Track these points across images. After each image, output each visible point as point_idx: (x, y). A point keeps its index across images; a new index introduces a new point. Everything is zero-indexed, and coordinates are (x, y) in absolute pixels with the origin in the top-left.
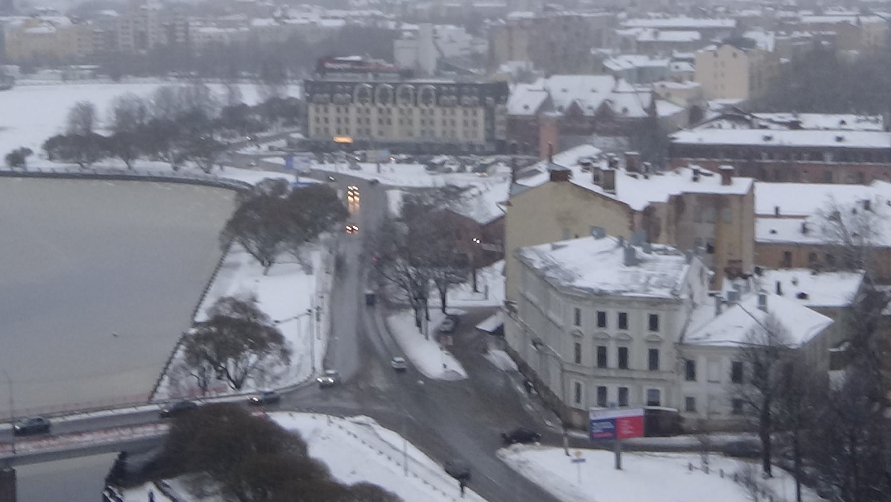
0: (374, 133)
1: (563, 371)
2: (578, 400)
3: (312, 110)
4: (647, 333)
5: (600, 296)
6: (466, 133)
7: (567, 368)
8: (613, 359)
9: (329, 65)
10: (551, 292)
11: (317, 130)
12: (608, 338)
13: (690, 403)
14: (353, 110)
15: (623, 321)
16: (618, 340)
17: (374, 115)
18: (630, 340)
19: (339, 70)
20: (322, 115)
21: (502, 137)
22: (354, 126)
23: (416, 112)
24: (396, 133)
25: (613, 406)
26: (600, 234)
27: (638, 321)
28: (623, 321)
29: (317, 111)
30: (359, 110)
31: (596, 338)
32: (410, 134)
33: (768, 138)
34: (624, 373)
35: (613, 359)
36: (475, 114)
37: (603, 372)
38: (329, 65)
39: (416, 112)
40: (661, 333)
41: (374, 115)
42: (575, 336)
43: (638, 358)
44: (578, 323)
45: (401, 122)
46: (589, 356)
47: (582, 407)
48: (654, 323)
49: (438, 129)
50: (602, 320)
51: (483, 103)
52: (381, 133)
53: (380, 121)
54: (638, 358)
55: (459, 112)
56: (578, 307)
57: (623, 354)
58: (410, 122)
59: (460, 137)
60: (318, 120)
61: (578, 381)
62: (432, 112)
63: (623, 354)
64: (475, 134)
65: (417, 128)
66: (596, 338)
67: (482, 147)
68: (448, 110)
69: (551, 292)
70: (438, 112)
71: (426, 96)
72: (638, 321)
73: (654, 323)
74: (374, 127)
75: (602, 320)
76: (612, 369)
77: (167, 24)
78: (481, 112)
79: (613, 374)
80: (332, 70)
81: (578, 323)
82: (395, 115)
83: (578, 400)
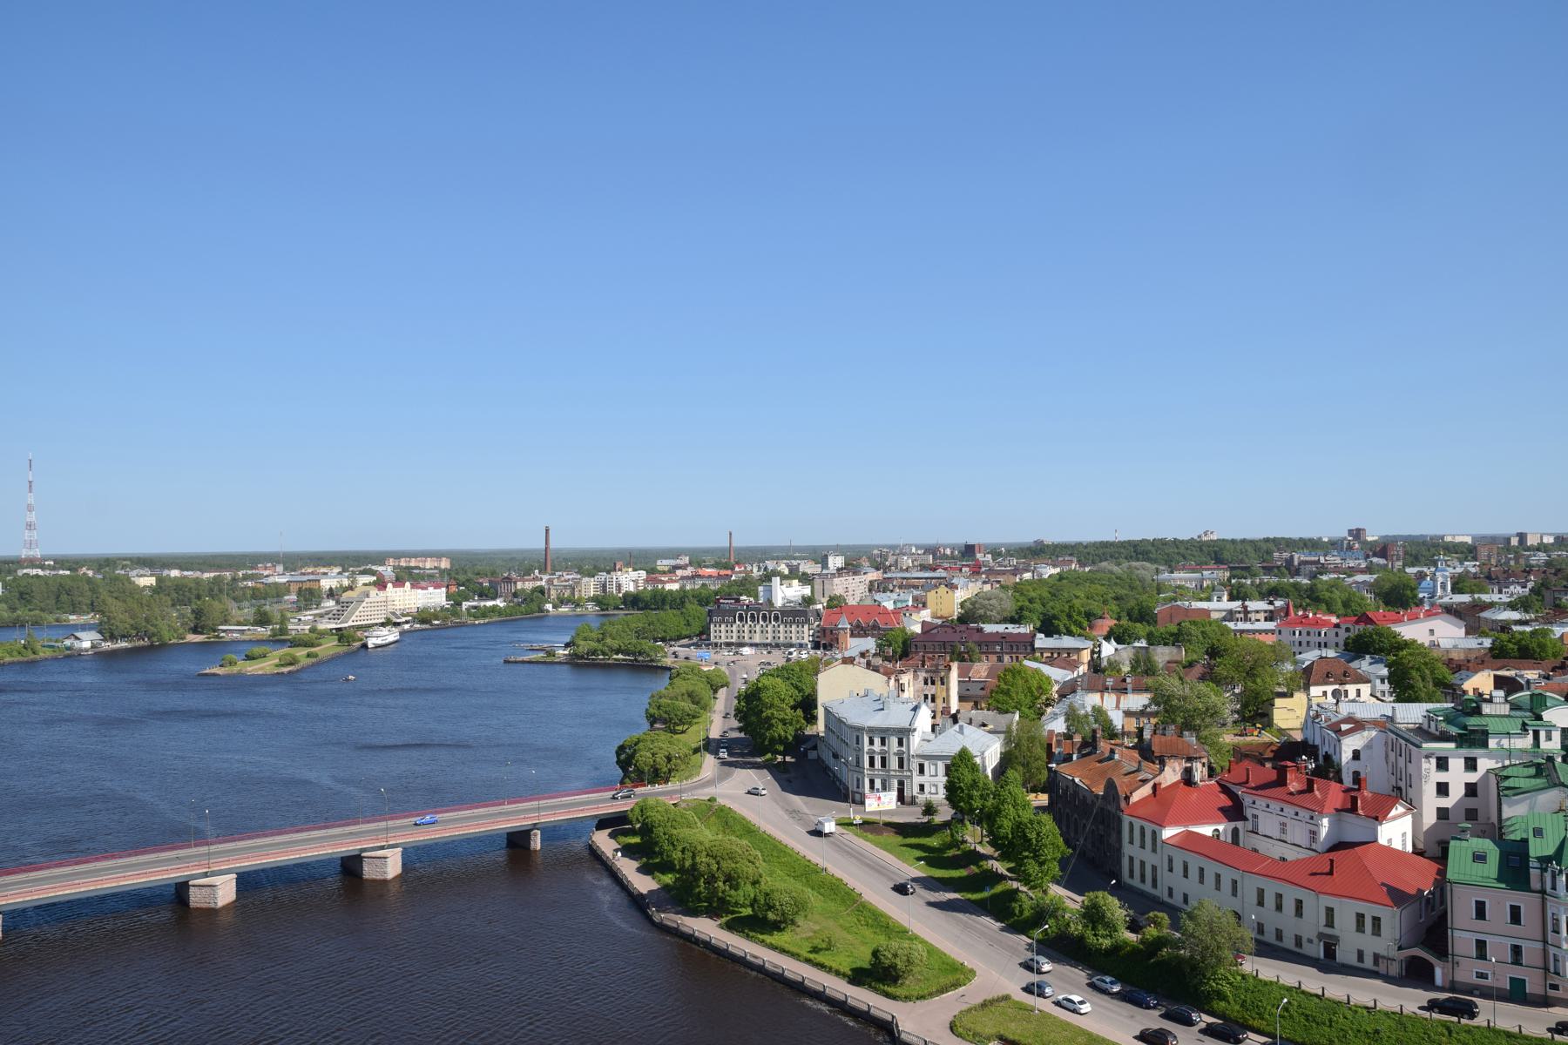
2: (858, 787)
3: (712, 626)
8: (878, 764)
9: (721, 601)
13: (922, 787)
16: (880, 753)
17: (746, 628)
22: (735, 635)
24: (757, 639)
25: (878, 790)
35: (878, 764)
38: (721, 601)
43: (894, 763)
44: (858, 743)
45: (762, 632)
47: (860, 791)
53: (750, 632)
54: (894, 763)
59: (794, 641)
62: (779, 626)
65: (770, 635)
81: (858, 743)
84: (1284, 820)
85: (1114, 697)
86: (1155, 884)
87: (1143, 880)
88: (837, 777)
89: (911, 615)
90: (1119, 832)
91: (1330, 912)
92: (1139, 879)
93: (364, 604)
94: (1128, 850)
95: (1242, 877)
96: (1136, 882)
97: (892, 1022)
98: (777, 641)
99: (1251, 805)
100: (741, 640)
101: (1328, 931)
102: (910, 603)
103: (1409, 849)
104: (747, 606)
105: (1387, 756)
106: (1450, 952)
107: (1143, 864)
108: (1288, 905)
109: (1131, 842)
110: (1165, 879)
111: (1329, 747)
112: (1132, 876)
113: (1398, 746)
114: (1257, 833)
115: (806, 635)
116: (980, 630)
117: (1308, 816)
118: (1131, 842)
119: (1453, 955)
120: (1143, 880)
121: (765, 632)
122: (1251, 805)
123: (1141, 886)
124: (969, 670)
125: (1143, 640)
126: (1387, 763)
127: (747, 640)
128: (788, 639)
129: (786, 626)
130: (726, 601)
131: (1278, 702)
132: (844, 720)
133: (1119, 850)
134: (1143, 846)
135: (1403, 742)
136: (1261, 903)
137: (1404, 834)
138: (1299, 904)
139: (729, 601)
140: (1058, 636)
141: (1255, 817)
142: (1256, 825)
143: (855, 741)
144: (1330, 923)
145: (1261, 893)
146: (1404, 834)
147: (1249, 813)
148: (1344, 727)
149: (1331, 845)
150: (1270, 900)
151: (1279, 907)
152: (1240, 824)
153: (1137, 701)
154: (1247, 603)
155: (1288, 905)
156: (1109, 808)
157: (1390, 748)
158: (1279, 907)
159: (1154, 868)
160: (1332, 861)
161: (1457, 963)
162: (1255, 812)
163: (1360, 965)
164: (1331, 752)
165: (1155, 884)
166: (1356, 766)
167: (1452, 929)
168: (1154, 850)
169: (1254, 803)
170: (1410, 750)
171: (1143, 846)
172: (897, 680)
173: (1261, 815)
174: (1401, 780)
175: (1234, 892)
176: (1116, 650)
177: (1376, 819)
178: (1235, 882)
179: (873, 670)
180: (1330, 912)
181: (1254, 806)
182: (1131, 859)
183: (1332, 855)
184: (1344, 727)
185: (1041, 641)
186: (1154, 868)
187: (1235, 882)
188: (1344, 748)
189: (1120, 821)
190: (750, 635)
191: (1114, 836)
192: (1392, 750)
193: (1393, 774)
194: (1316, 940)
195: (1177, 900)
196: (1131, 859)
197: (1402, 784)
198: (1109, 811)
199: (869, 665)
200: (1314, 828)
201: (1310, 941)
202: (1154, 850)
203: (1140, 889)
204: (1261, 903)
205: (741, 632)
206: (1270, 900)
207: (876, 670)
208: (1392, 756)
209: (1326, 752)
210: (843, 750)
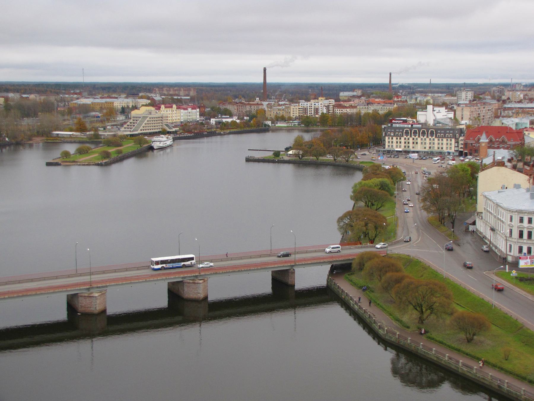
0: (411, 148)
1: (506, 240)
3: (387, 138)
5: (520, 212)
6: (447, 148)
7: (508, 239)
10: (500, 209)
11: (389, 146)
12: (524, 228)
14: (403, 138)
17: (411, 140)
19: (397, 123)
20: (390, 140)
21: (462, 150)
22: (403, 145)
23: (428, 139)
24: (419, 148)
25: (525, 254)
29: (389, 138)
30: (405, 139)
31: (518, 227)
32: (425, 148)
34: (529, 242)
36: (451, 140)
37: (521, 241)
38: (393, 121)
39: (428, 139)
41: (411, 140)
42: (510, 226)
45: (422, 143)
46: (516, 234)
47: (512, 254)
49: (436, 146)
50: (521, 220)
51: (454, 137)
52: (413, 147)
53: (413, 143)
55: (445, 140)
56: (511, 215)
58: (425, 143)
59: (445, 150)
60: (389, 142)
61: (511, 244)
62: (434, 140)
64: (451, 148)
65: (428, 146)
66: (518, 227)
67: (453, 153)
68: (449, 139)
69: (499, 208)
70: (436, 140)
71: (432, 134)
74: (411, 145)
75: (521, 220)
76: (525, 240)
77: (326, 105)
78: (453, 140)
79: (525, 241)
80: (395, 123)
82: (419, 140)
83: (510, 251)
88: (493, 244)
89: (529, 134)
93: (148, 119)
98: (431, 150)
100: (407, 149)
102: (528, 126)
104: (412, 125)
115: (453, 146)
121: (423, 143)
127: (411, 149)
128: (440, 149)
130: (397, 121)
139: (399, 122)
190: (414, 145)
199: (514, 168)
205: (407, 143)
207: (520, 171)
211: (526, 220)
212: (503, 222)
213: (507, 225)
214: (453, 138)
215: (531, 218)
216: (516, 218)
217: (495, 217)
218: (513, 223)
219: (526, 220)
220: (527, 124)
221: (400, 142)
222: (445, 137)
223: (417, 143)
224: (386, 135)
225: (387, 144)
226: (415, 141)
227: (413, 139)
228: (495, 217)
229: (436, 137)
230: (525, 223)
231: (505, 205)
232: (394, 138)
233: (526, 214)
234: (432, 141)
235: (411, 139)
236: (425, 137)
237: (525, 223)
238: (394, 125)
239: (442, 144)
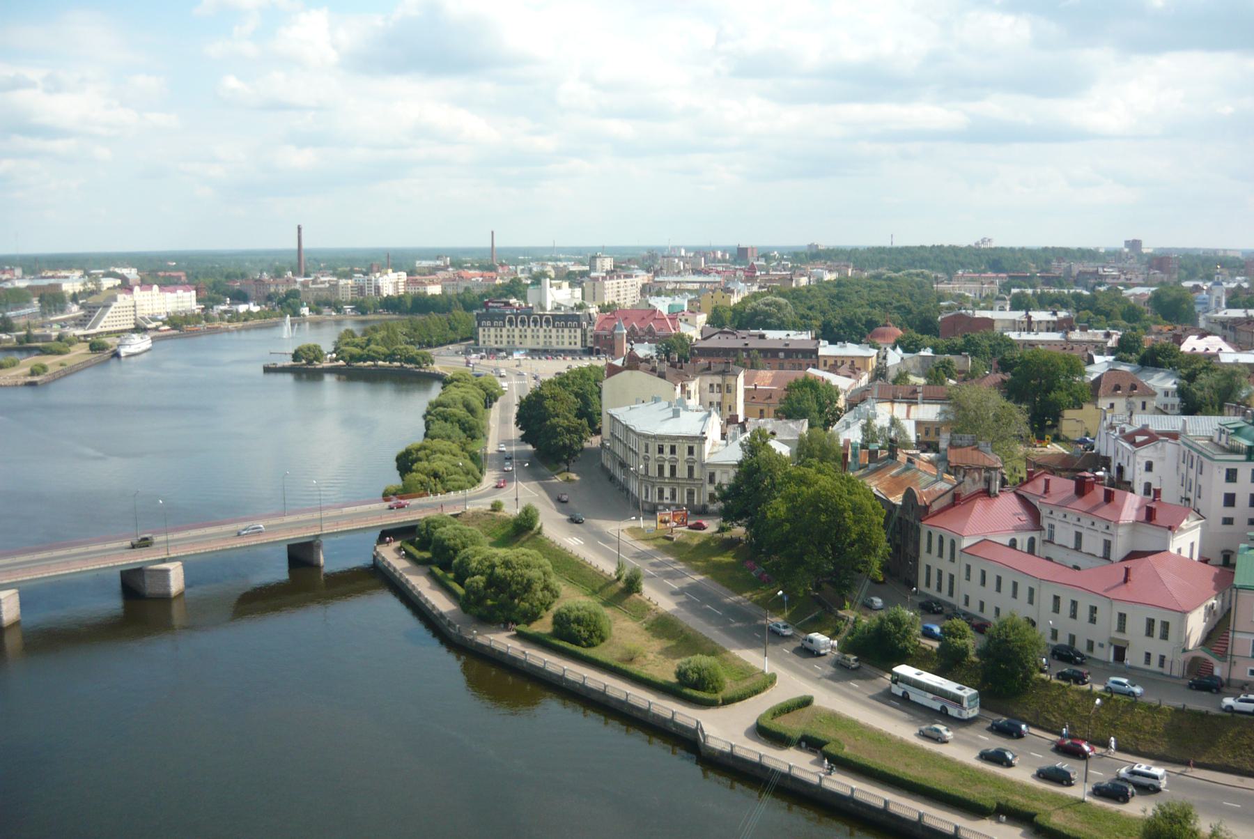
0: (517, 343)
2: (647, 497)
3: (481, 330)
4: (686, 456)
8: (667, 473)
9: (490, 304)
12: (664, 460)
14: (504, 330)
15: (673, 450)
17: (517, 332)
18: (677, 460)
19: (496, 307)
21: (592, 345)
22: (505, 339)
23: (541, 331)
25: (667, 498)
26: (656, 400)
27: (682, 453)
28: (673, 450)
29: (484, 330)
30: (508, 330)
31: (656, 460)
32: (538, 344)
33: (746, 344)
35: (667, 473)
36: (575, 331)
38: (490, 304)
39: (541, 331)
40: (695, 457)
42: (645, 459)
44: (647, 452)
45: (533, 337)
48: (691, 451)
49: (554, 340)
52: (521, 343)
53: (521, 336)
54: (682, 472)
55: (566, 330)
57: (673, 469)
58: (538, 337)
62: (550, 331)
63: (673, 469)
64: (575, 343)
65: (542, 340)
70: (554, 331)
72: (682, 453)
73: (691, 451)
74: (517, 340)
75: (661, 450)
78: (579, 331)
79: (667, 481)
80: (492, 307)
81: (647, 452)
82: (529, 333)
83: (647, 497)
84: (1079, 530)
85: (905, 406)
86: (951, 594)
87: (939, 589)
90: (917, 544)
91: (1122, 617)
92: (936, 588)
93: (112, 309)
94: (925, 559)
95: (1040, 586)
96: (932, 591)
97: (697, 728)
99: (1049, 515)
101: (1119, 636)
103: (1196, 557)
105: (1178, 467)
106: (1229, 652)
107: (940, 573)
108: (1083, 612)
109: (929, 551)
110: (962, 587)
111: (1123, 457)
112: (928, 584)
113: (1190, 458)
114: (1053, 543)
116: (762, 337)
117: (1104, 527)
118: (929, 551)
119: (1232, 655)
120: (939, 589)
122: (1049, 515)
123: (937, 595)
124: (754, 377)
125: (928, 348)
126: (1178, 474)
129: (558, 331)
130: (495, 305)
131: (1068, 413)
132: (633, 428)
133: (916, 559)
134: (941, 555)
135: (1195, 454)
136: (1056, 609)
137: (1192, 544)
138: (1093, 610)
139: (498, 305)
140: (841, 343)
141: (1052, 526)
142: (1052, 534)
143: (644, 449)
144: (1122, 628)
145: (1056, 599)
146: (1192, 544)
147: (1045, 523)
148: (1139, 439)
149: (1129, 552)
150: (1065, 607)
151: (1074, 615)
152: (1036, 535)
153: (929, 412)
154: (1030, 313)
155: (1083, 612)
156: (907, 518)
157: (1181, 460)
158: (1074, 615)
159: (952, 577)
160: (1127, 570)
161: (1235, 663)
162: (1053, 522)
163: (1146, 667)
164: (1124, 464)
165: (951, 594)
166: (1148, 477)
167: (1234, 631)
168: (952, 559)
169: (1051, 513)
170: (1202, 462)
171: (941, 555)
172: (683, 387)
173: (1058, 525)
174: (1190, 490)
175: (1031, 602)
176: (902, 359)
177: (1170, 528)
178: (1031, 591)
179: (659, 376)
180: (1122, 617)
181: (1051, 516)
182: (928, 568)
183: (1128, 564)
184: (1139, 439)
185: (826, 349)
186: (952, 577)
187: (1031, 591)
188: (1138, 459)
189: (918, 530)
191: (911, 547)
192: (1184, 462)
193: (1182, 485)
194: (1106, 645)
195: (974, 608)
196: (928, 568)
197: (1191, 495)
198: (907, 521)
200: (1108, 538)
201: (1101, 645)
202: (952, 559)
203: (936, 598)
204: (1056, 609)
206: (1065, 607)
208: (1183, 468)
209: (1119, 464)
210: (631, 460)
211: (667, 450)
212: (636, 453)
213: (641, 457)
214: (579, 327)
215: (675, 446)
216: (653, 447)
217: (625, 445)
218: (649, 455)
219: (667, 450)
220: (683, 306)
221: (501, 336)
222: (566, 327)
223: (526, 336)
224: (479, 325)
225: (481, 339)
226: (523, 334)
227: (521, 330)
228: (625, 445)
229: (554, 326)
230: (667, 454)
231: (638, 430)
232: (492, 330)
233: (667, 440)
234: (548, 334)
235: (517, 331)
236: (538, 327)
237: (667, 454)
238: (491, 310)
239: (563, 337)
